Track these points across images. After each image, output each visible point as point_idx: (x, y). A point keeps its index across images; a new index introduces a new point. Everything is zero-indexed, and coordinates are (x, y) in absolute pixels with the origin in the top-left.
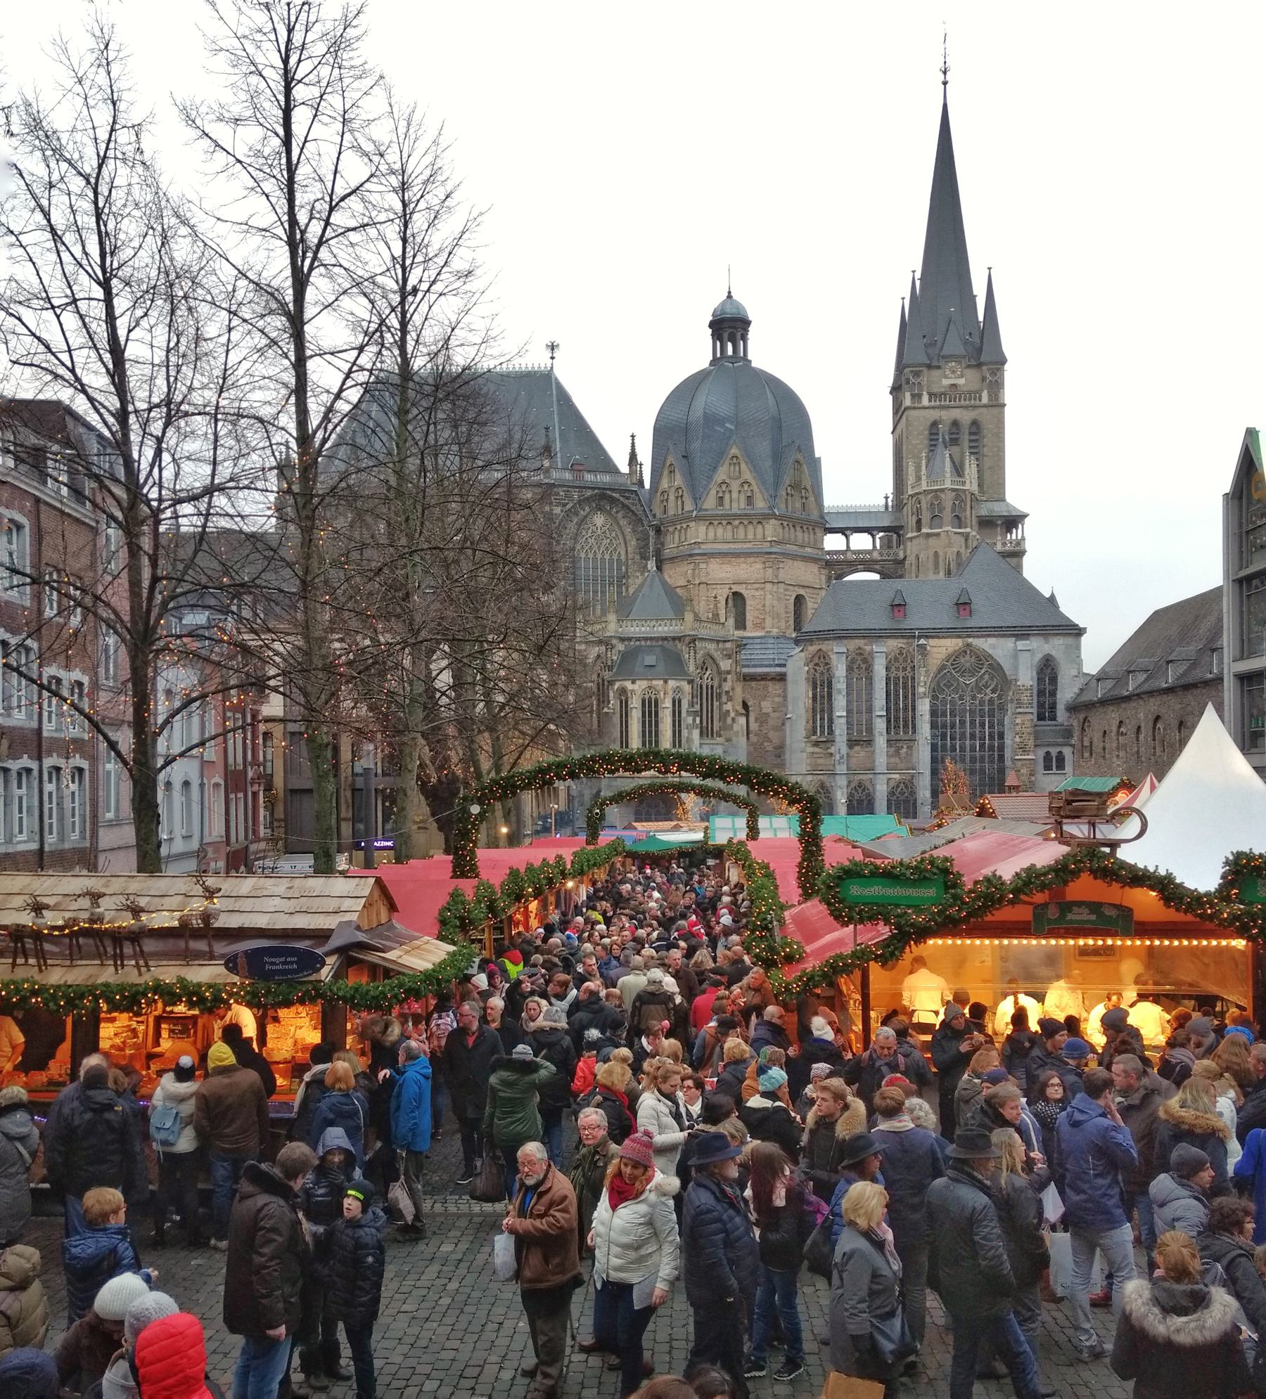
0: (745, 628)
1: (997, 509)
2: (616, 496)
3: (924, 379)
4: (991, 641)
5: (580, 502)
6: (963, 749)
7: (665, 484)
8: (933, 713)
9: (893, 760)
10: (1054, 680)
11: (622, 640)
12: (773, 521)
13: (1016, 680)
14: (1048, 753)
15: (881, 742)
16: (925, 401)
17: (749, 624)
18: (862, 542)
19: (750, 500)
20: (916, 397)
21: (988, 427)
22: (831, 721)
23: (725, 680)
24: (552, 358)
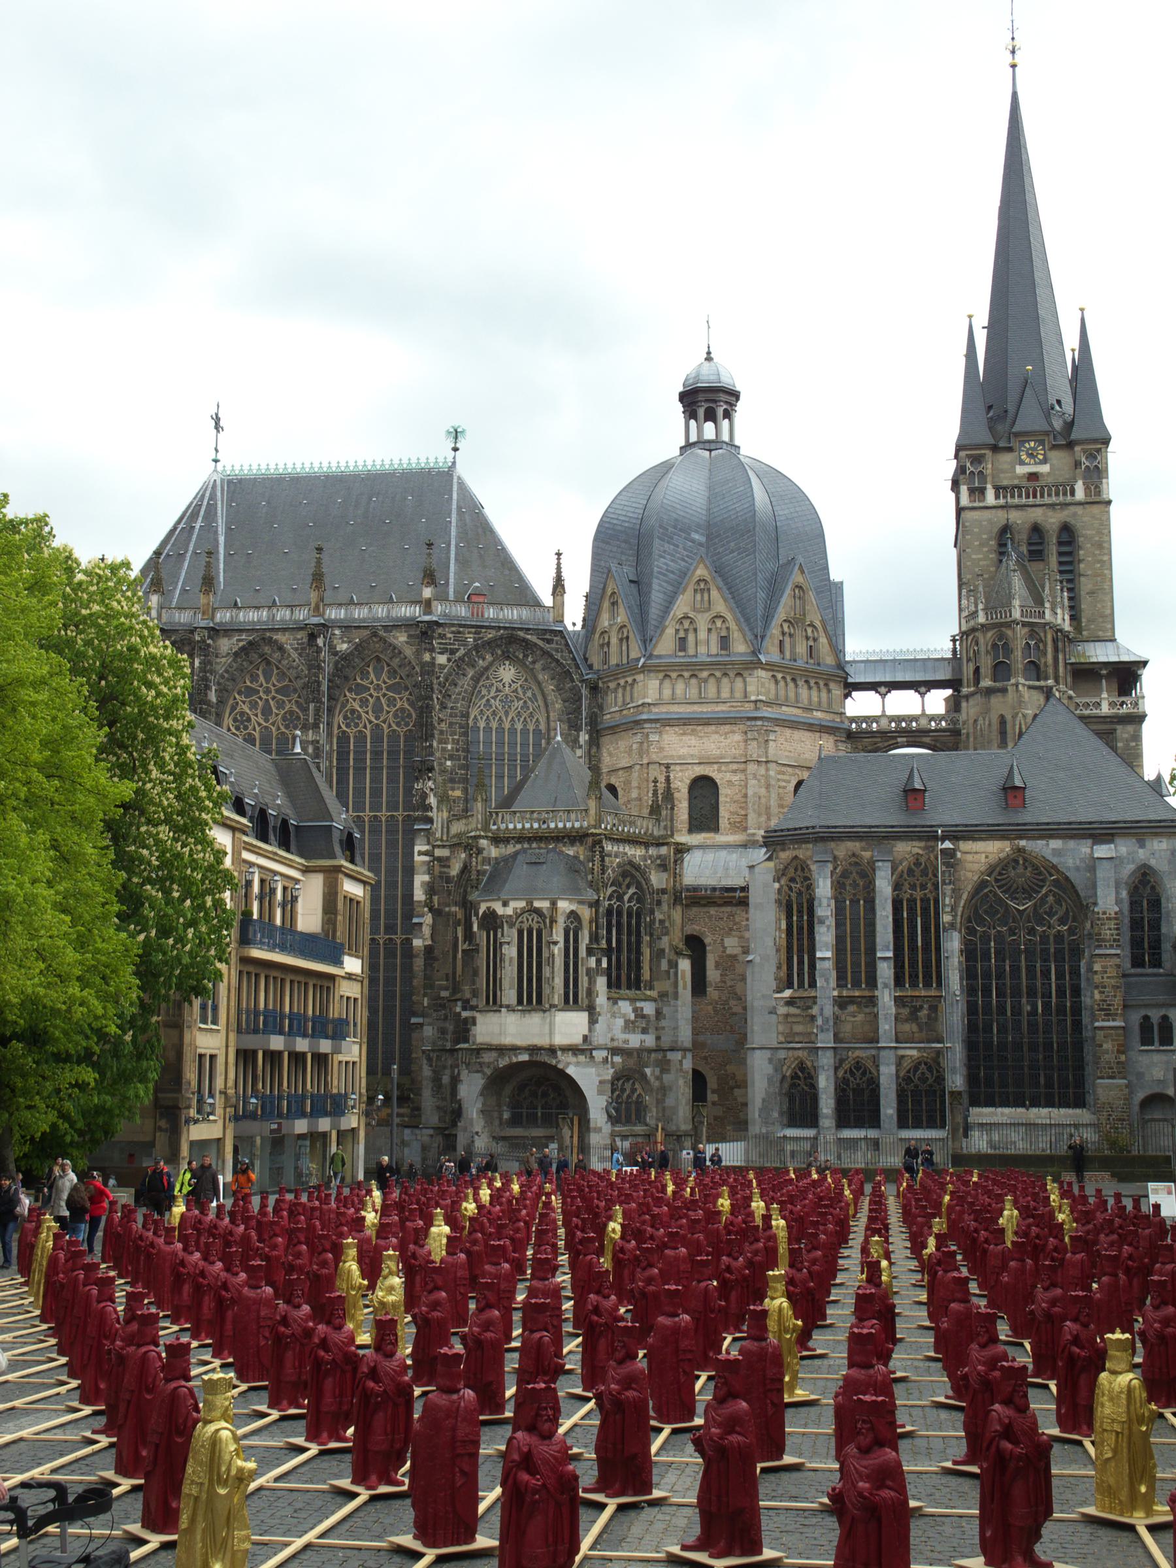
0: (716, 829)
1: (1100, 654)
2: (530, 643)
3: (988, 468)
4: (1056, 844)
5: (476, 648)
6: (1017, 1011)
7: (605, 621)
8: (969, 952)
9: (907, 1027)
10: (1156, 904)
11: (497, 840)
12: (762, 673)
13: (1095, 904)
14: (1146, 1018)
15: (886, 998)
16: (990, 498)
17: (723, 823)
18: (903, 703)
19: (725, 642)
20: (978, 492)
21: (1086, 532)
22: (812, 966)
23: (659, 903)
24: (455, 449)
